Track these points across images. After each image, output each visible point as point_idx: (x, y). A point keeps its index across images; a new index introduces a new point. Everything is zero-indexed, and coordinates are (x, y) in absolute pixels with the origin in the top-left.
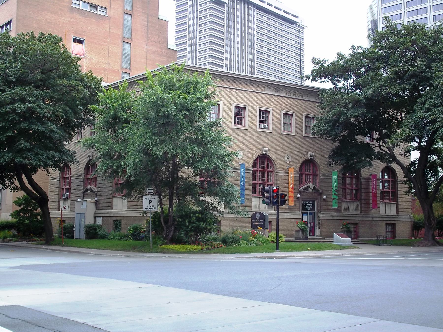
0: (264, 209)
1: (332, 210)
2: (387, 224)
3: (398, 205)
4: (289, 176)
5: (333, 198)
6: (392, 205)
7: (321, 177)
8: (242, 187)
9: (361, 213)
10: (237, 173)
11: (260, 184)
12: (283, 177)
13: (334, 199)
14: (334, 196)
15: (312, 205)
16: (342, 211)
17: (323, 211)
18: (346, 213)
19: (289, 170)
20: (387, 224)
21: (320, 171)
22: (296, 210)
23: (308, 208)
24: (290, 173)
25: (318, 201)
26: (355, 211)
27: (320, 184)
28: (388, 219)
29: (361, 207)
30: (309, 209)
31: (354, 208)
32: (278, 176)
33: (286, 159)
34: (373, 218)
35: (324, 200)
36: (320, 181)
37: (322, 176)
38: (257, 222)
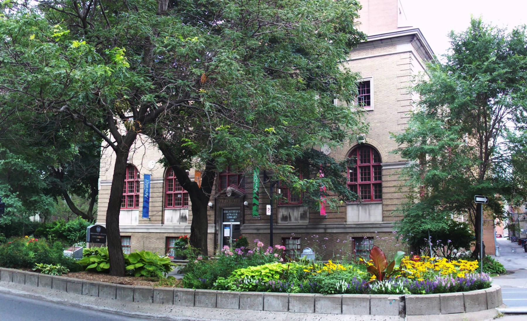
0: (177, 223)
6: (373, 207)
8: (145, 199)
15: (237, 214)
16: (280, 221)
18: (286, 223)
23: (231, 219)
28: (356, 230)
30: (233, 220)
31: (300, 215)
38: (99, 235)
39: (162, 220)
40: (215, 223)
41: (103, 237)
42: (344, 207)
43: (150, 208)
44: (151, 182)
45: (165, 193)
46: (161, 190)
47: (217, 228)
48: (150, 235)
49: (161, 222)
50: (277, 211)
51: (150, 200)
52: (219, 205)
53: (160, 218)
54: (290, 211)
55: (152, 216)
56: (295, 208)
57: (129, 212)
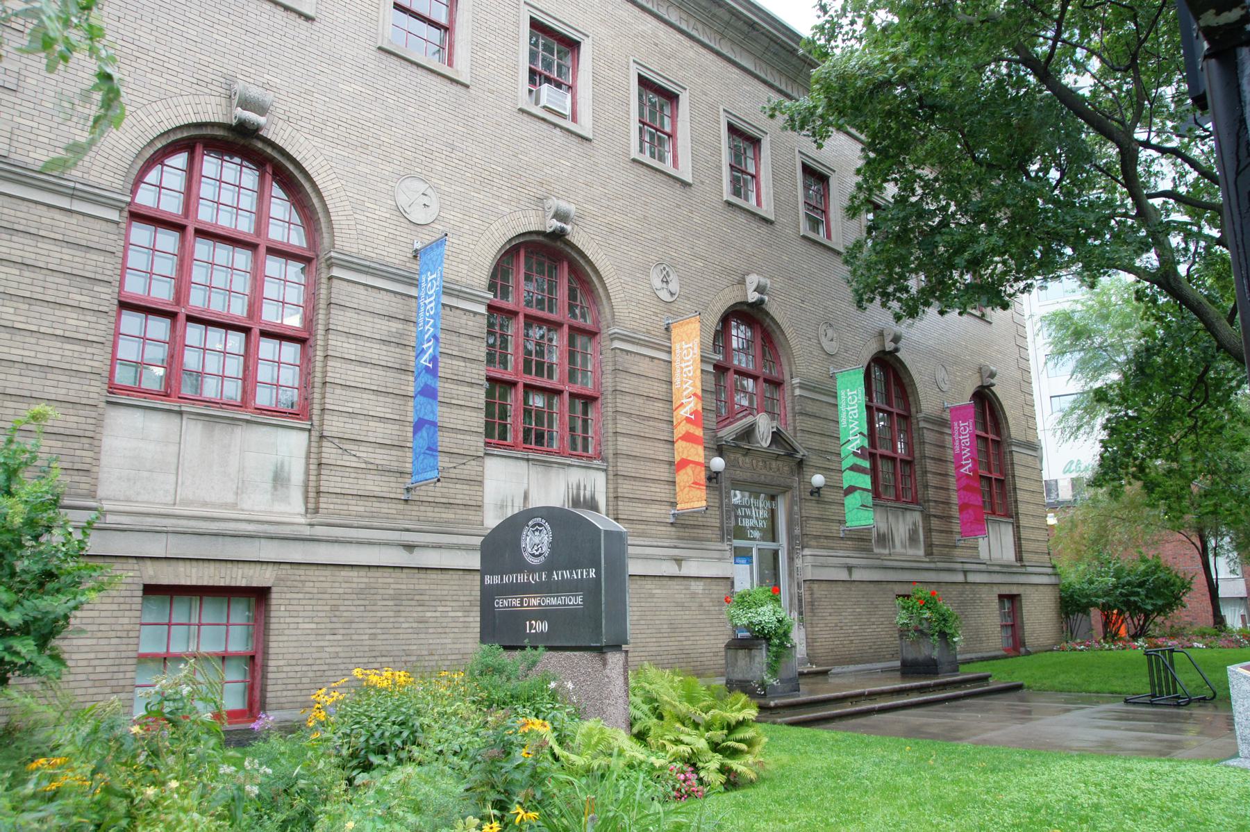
1: (842, 538)
2: (1001, 597)
3: (1018, 527)
4: (676, 365)
5: (845, 486)
6: (1003, 527)
7: (797, 392)
9: (929, 553)
10: (398, 299)
11: (529, 388)
12: (644, 367)
13: (851, 490)
14: (850, 479)
17: (813, 543)
19: (674, 332)
20: (1001, 597)
21: (790, 365)
22: (708, 533)
24: (676, 347)
25: (793, 496)
27: (794, 421)
29: (928, 531)
32: (623, 359)
33: (657, 283)
34: (965, 572)
35: (816, 491)
36: (793, 408)
37: (802, 386)
38: (525, 589)
41: (576, 601)
48: (423, 583)
57: (219, 431)
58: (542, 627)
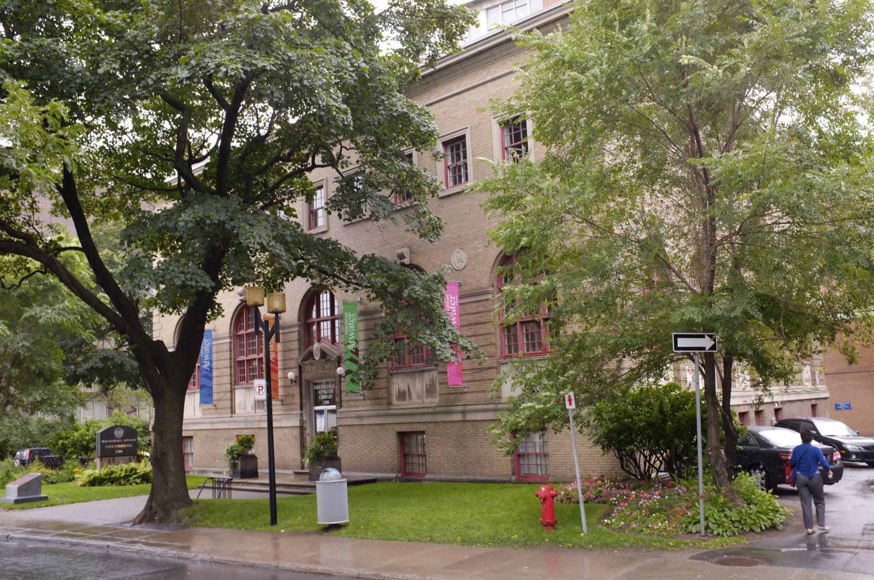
11: (250, 361)
16: (395, 401)
18: (405, 404)
26: (427, 396)
30: (328, 402)
34: (463, 412)
38: (120, 443)
39: (232, 408)
40: (301, 409)
42: (496, 368)
43: (215, 388)
44: (214, 343)
45: (235, 359)
46: (227, 355)
47: (305, 418)
49: (229, 411)
50: (388, 382)
51: (215, 373)
52: (306, 376)
53: (228, 404)
54: (409, 380)
55: (219, 400)
56: (417, 375)
58: (121, 451)
